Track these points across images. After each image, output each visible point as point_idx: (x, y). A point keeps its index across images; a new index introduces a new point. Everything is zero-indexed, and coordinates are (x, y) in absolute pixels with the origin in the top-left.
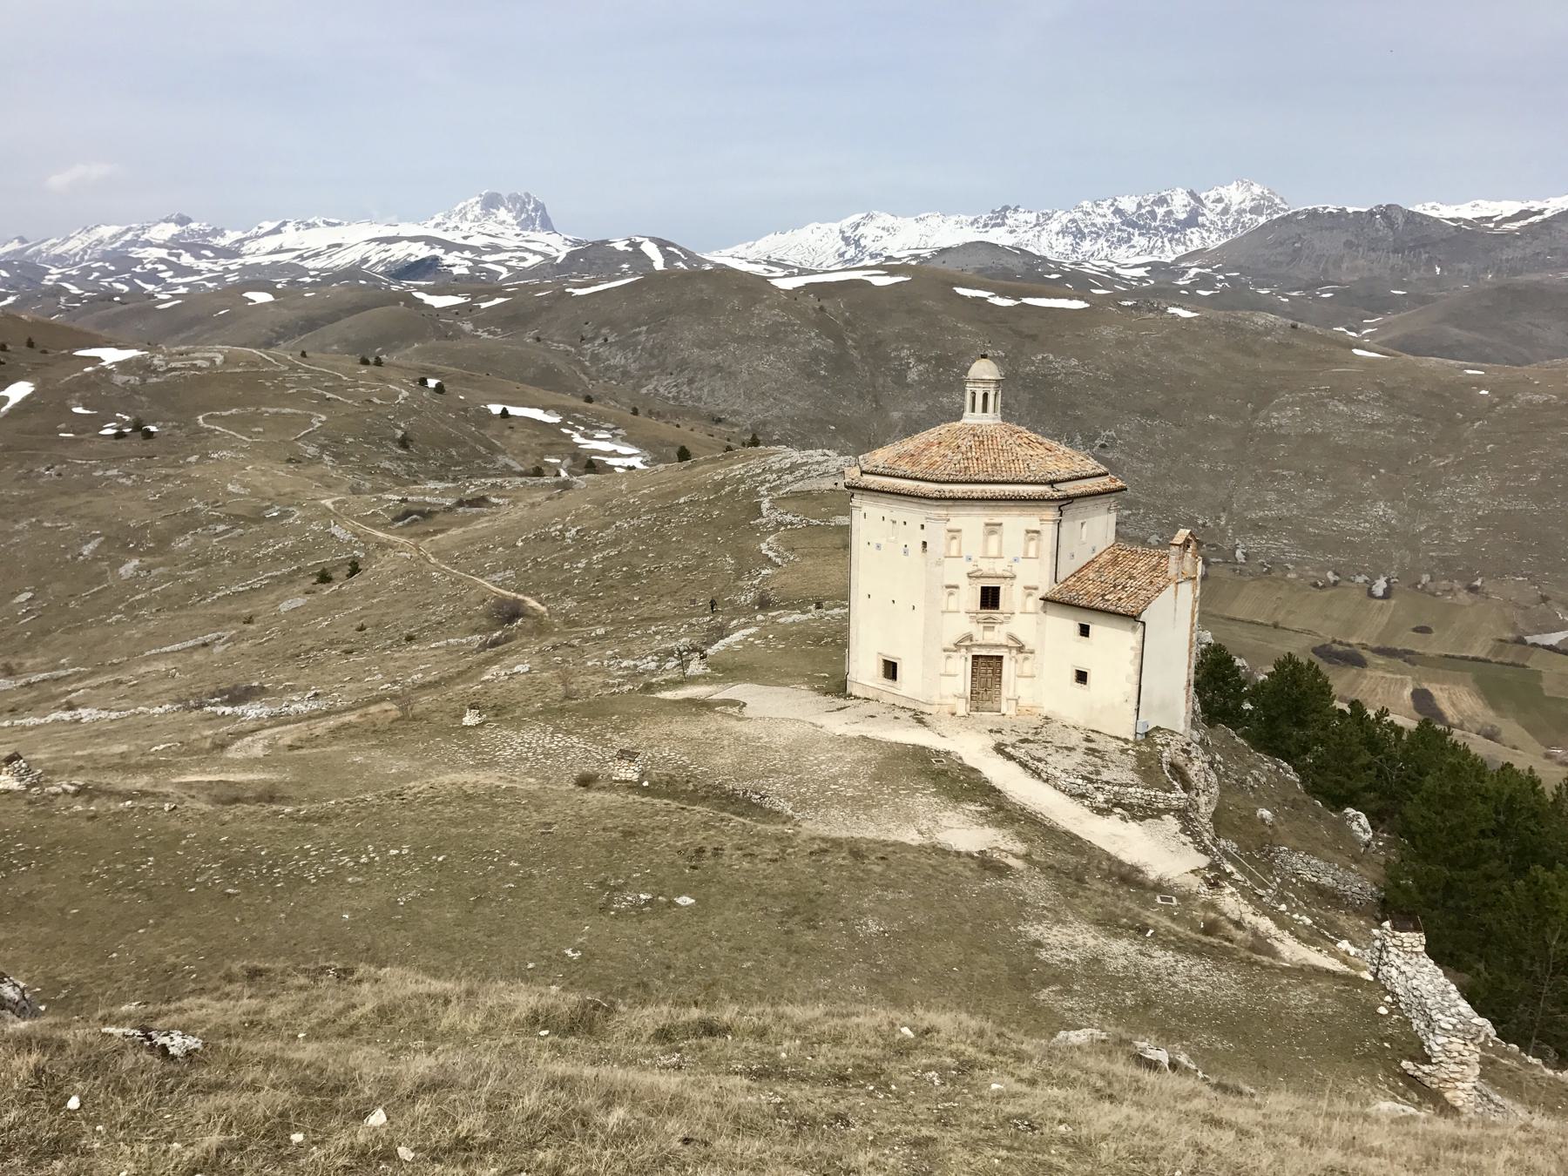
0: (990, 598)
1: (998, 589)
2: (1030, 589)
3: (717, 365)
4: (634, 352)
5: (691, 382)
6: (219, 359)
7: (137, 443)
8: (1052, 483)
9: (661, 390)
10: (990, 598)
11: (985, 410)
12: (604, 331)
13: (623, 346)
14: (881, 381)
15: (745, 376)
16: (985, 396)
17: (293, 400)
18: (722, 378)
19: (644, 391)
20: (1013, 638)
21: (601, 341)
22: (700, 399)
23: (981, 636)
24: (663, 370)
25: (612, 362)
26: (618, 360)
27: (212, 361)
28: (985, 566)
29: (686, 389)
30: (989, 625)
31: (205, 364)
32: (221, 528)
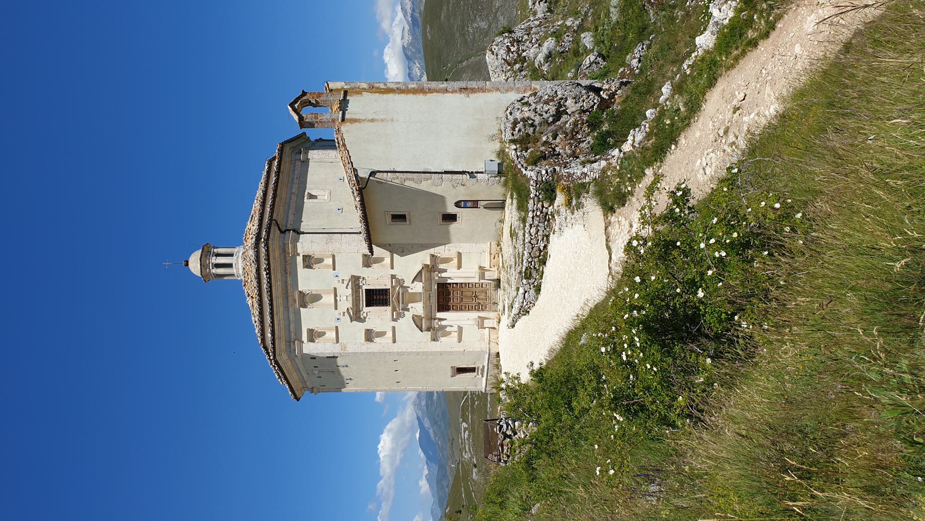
0: (377, 298)
1: (368, 292)
2: (368, 261)
6: (465, 425)
10: (377, 298)
23: (418, 308)
27: (465, 429)
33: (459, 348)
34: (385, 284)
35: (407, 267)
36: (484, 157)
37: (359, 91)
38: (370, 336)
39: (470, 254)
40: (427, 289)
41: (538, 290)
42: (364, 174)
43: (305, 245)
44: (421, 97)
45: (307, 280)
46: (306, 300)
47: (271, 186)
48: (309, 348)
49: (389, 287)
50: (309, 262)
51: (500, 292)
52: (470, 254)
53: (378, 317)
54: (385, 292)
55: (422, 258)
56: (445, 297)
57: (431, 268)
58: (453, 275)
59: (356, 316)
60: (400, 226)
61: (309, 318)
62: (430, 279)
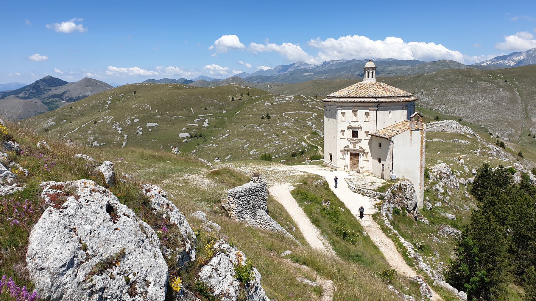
0: (355, 134)
2: (367, 132)
3: (462, 101)
4: (432, 97)
5: (451, 107)
6: (293, 98)
7: (266, 120)
8: (375, 98)
9: (440, 110)
10: (355, 134)
11: (368, 77)
12: (422, 90)
13: (427, 95)
14: (529, 107)
15: (472, 105)
16: (369, 73)
17: (309, 110)
18: (463, 106)
19: (434, 110)
20: (361, 148)
21: (420, 93)
22: (454, 113)
23: (351, 147)
24: (441, 102)
25: (424, 100)
26: (426, 99)
27: (290, 98)
28: (353, 125)
29: (449, 109)
30: (354, 143)
31: (288, 99)
32: (277, 142)
33: (338, 158)
34: (359, 137)
35: (364, 145)
36: (396, 174)
37: (422, 134)
38: (343, 131)
39: (367, 163)
40: (357, 150)
41: (355, 192)
42: (392, 139)
43: (372, 113)
44: (420, 153)
45: (361, 113)
46: (355, 112)
47: (393, 99)
48: (339, 112)
49: (358, 138)
50: (367, 114)
51: (356, 173)
52: (367, 163)
53: (349, 134)
54: (357, 137)
55: (367, 150)
56: (355, 155)
57: (364, 152)
58: (362, 158)
59: (349, 128)
60: (378, 145)
61: (349, 113)
62: (360, 151)
